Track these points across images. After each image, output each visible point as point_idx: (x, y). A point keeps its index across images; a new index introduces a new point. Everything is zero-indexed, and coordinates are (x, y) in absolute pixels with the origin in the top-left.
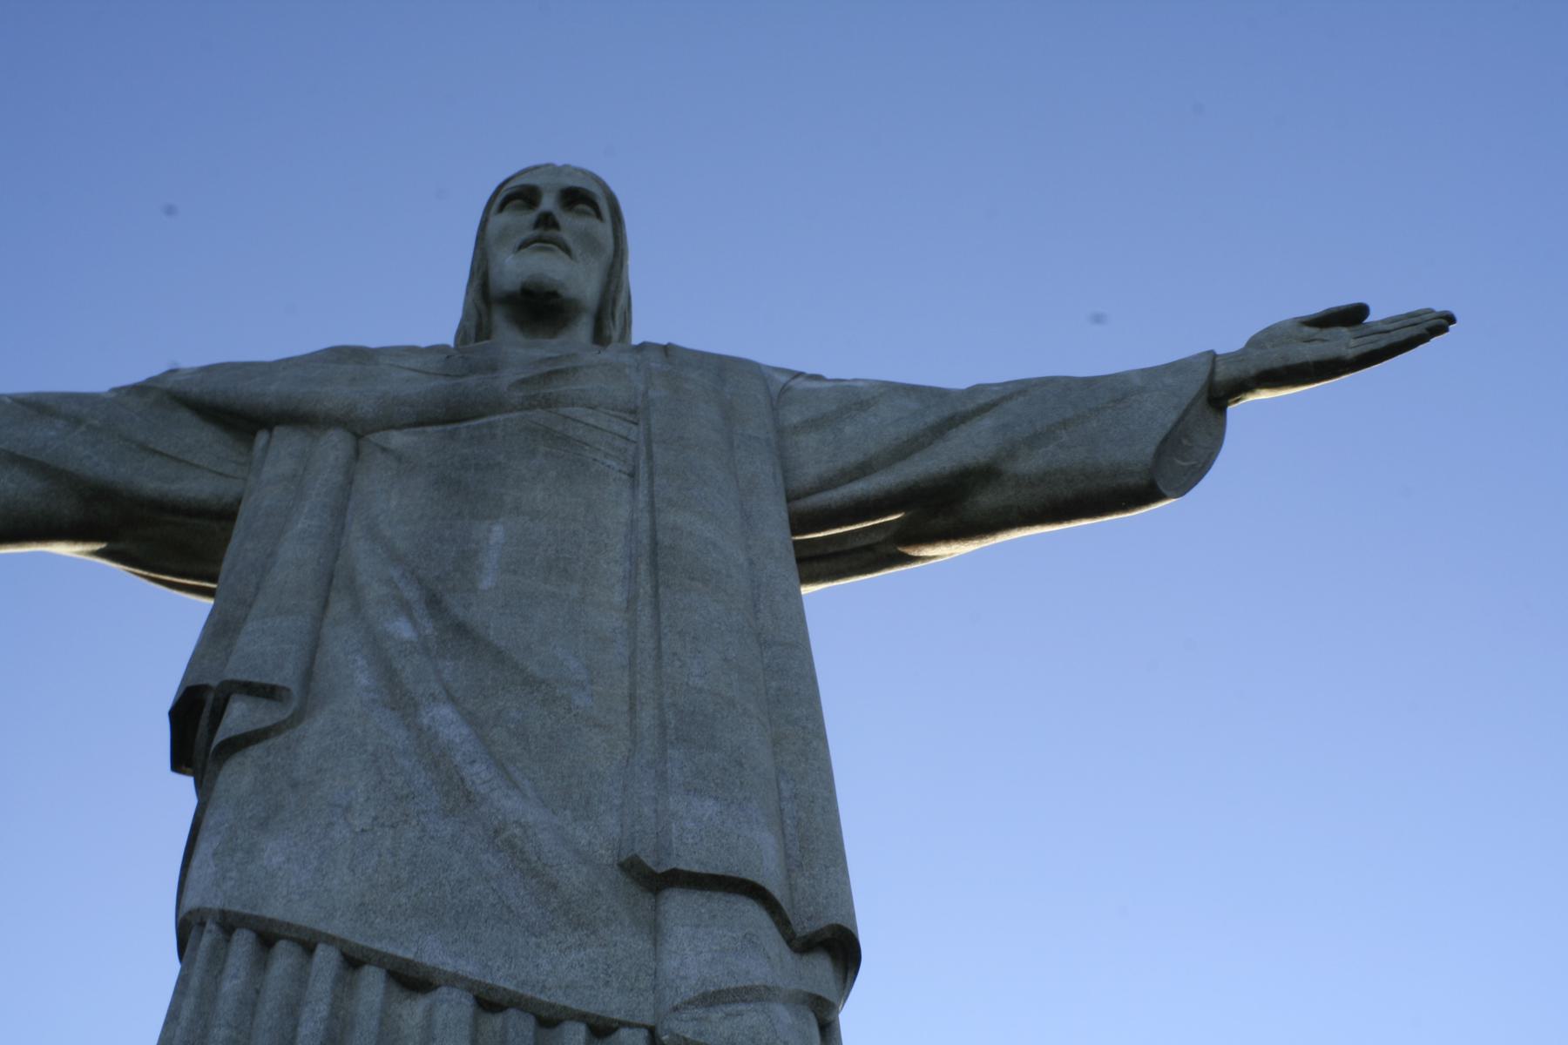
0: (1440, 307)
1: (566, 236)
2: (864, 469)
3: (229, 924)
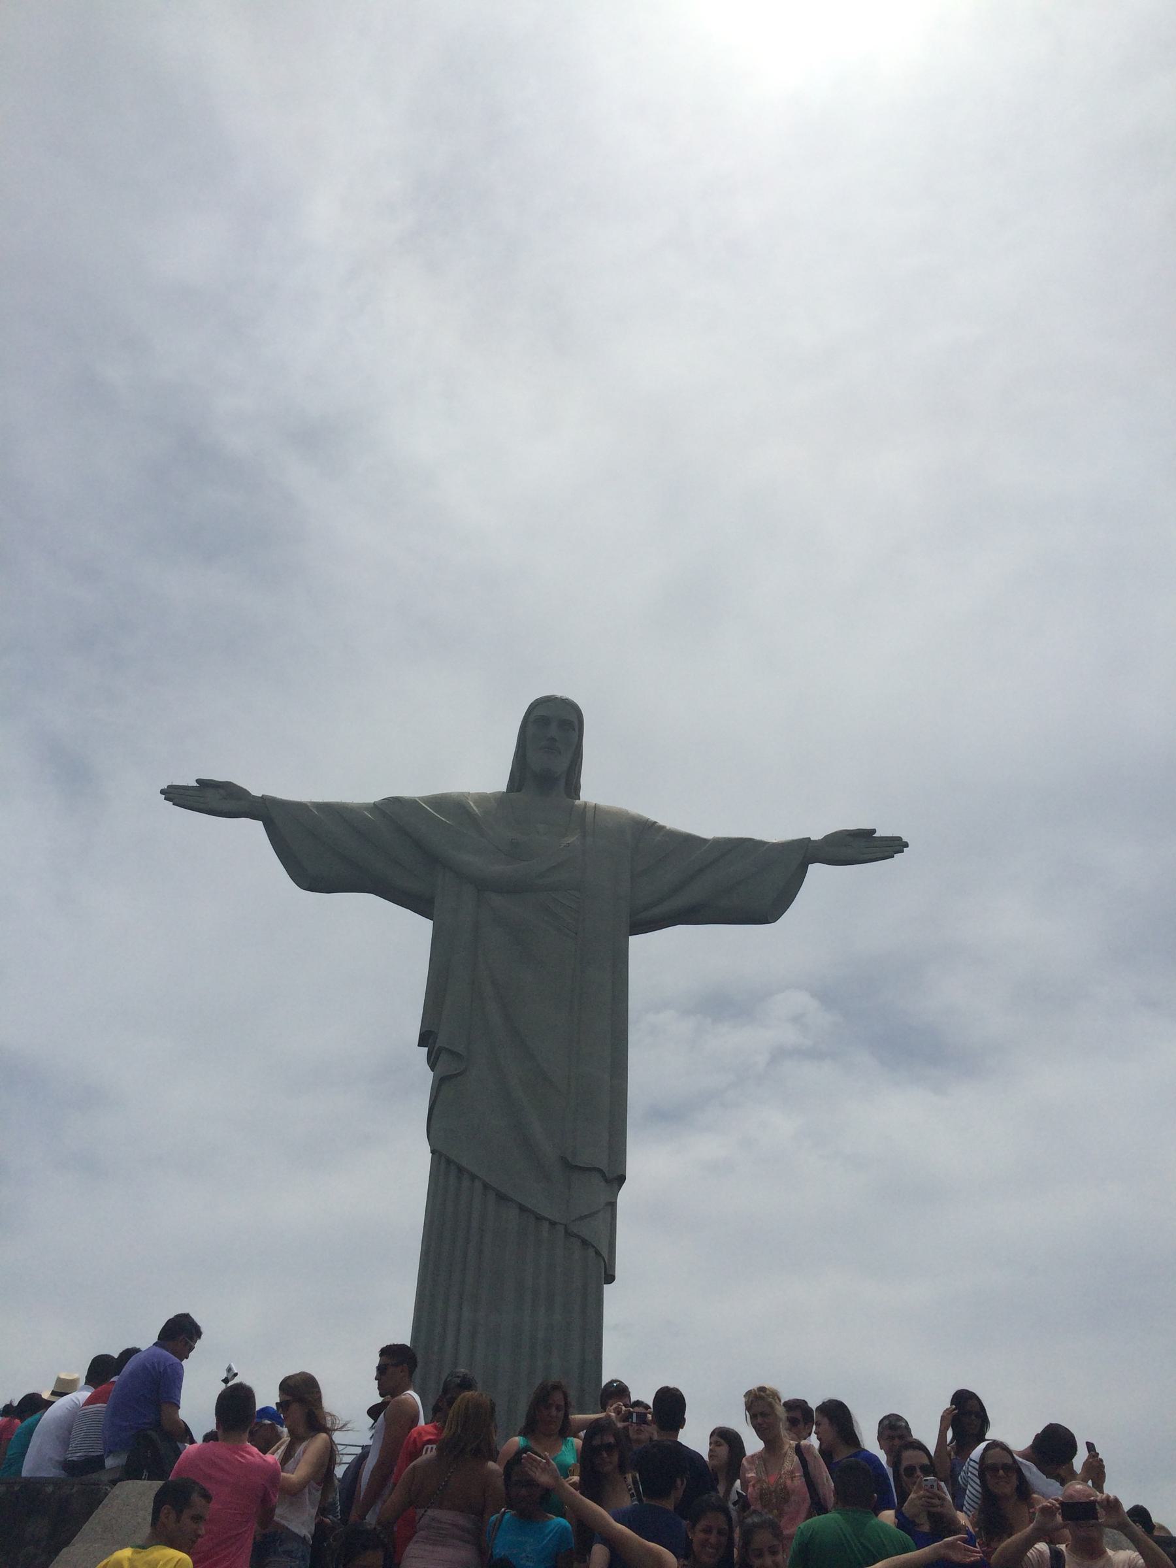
0: (905, 839)
3: (449, 1161)
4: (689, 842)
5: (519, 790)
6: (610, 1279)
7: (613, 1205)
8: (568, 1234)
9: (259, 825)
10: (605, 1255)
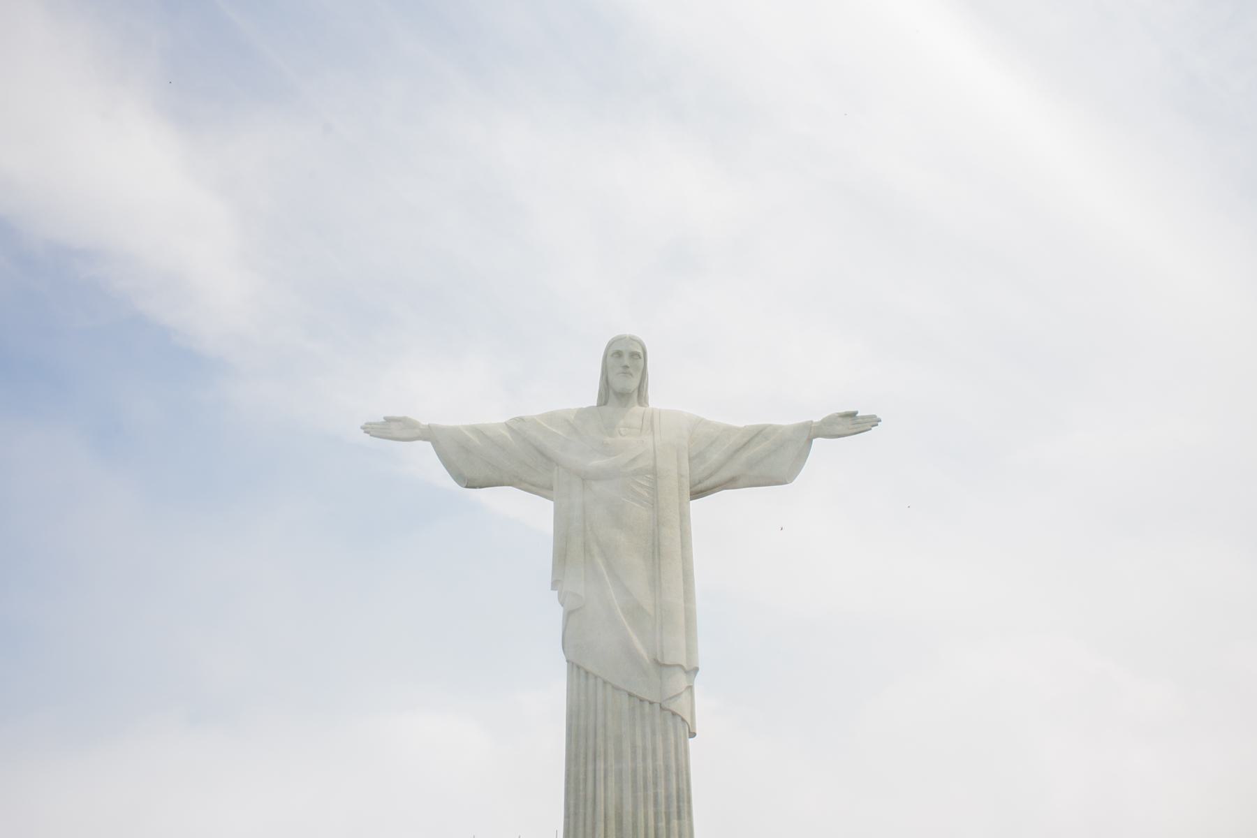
0: (879, 416)
1: (631, 370)
2: (711, 475)
3: (578, 667)
4: (729, 430)
5: (605, 404)
6: (693, 735)
7: (690, 688)
8: (662, 709)
9: (429, 444)
10: (688, 719)
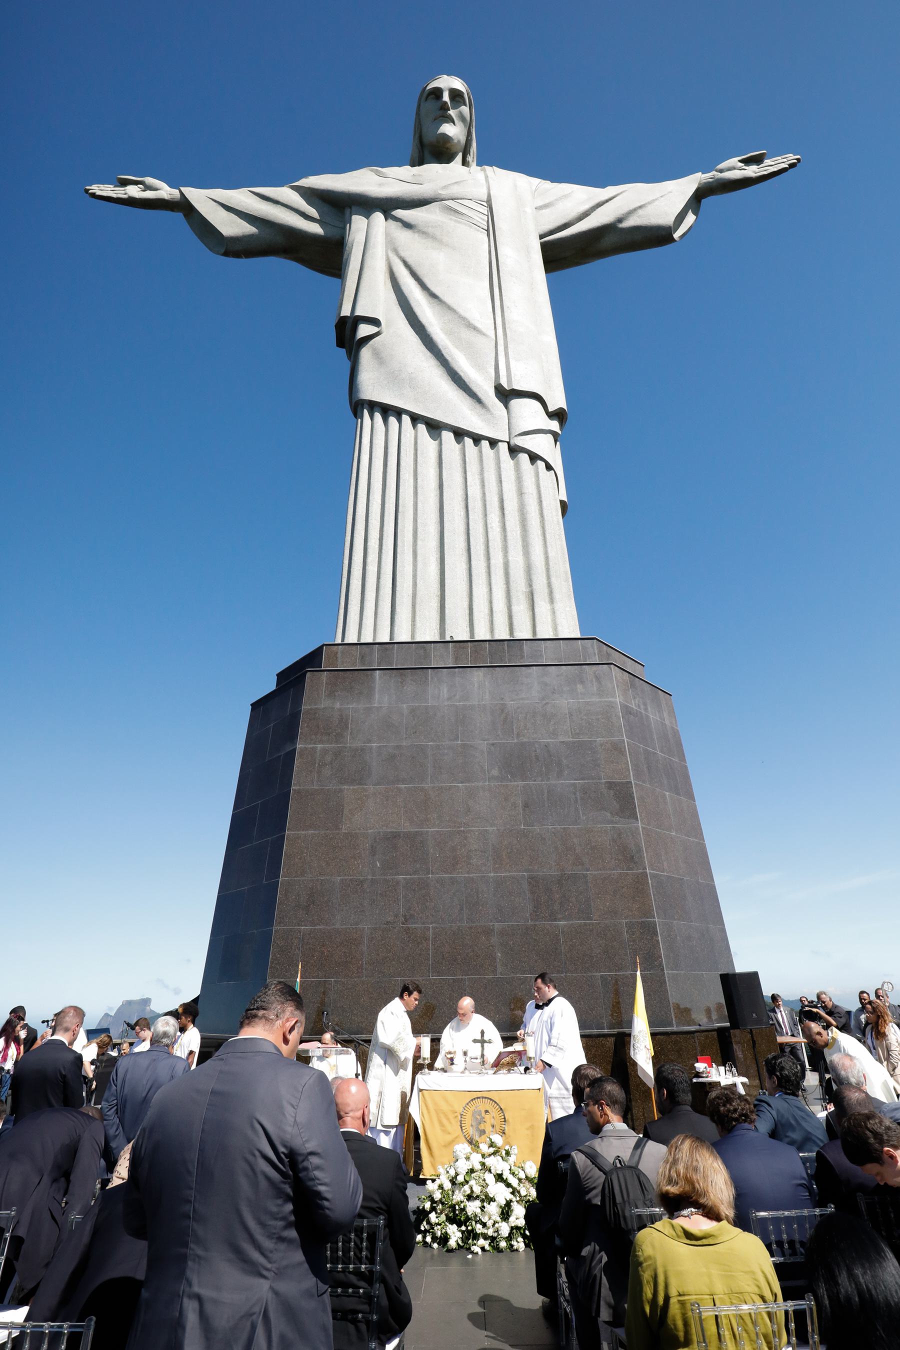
8: (514, 451)
9: (179, 216)
